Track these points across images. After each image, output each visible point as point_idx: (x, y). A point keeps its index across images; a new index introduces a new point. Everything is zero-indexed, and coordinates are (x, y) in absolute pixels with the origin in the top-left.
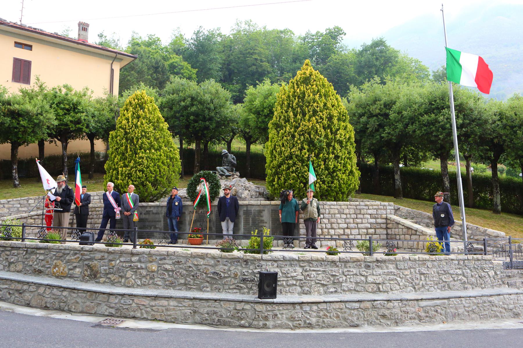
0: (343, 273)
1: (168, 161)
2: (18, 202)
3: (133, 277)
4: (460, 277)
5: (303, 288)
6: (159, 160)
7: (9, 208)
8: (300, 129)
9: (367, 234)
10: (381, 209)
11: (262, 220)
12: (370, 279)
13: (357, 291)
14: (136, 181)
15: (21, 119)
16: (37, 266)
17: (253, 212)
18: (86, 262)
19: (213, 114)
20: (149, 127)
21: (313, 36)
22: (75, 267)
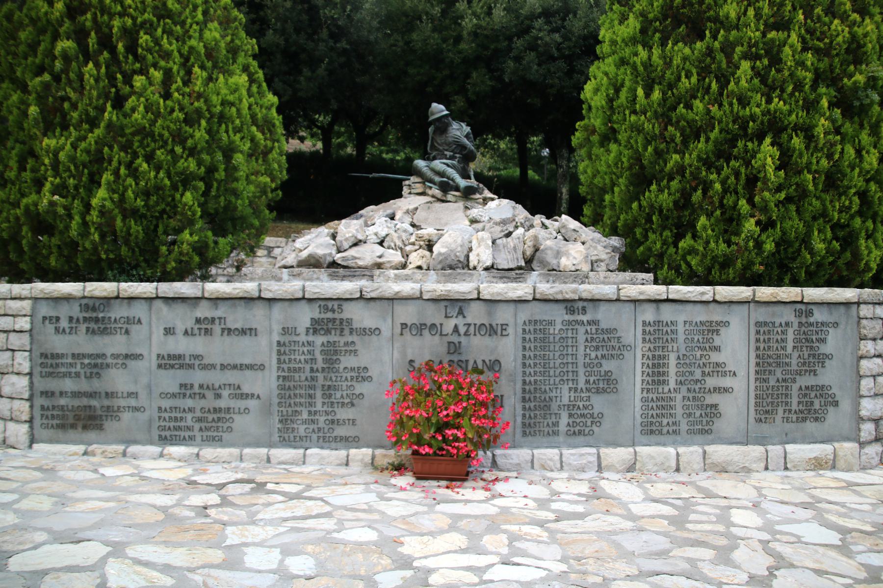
11: (718, 365)
17: (681, 328)
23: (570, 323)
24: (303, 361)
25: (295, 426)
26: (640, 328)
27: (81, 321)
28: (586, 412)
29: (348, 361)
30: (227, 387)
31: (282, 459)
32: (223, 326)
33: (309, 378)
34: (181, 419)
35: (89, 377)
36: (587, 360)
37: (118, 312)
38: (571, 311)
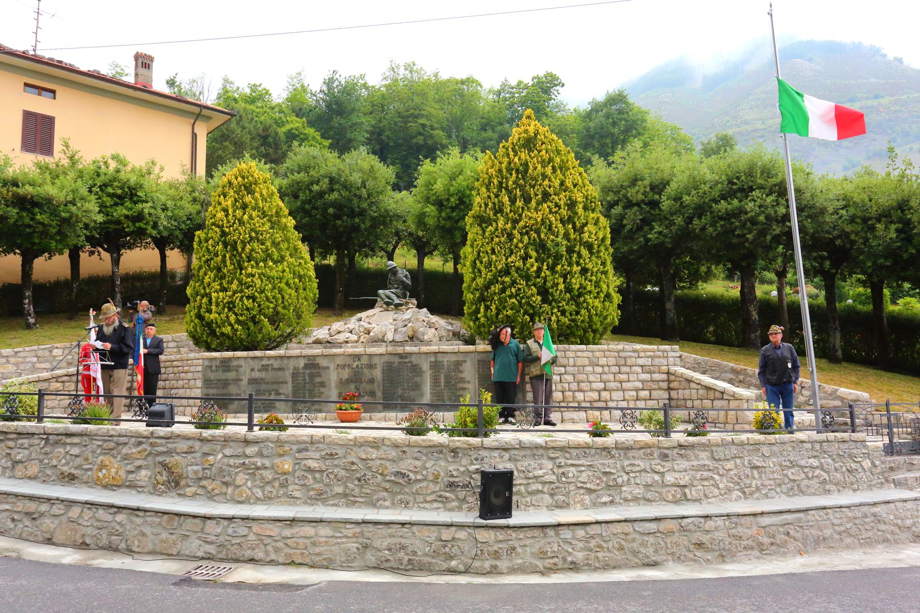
0: (623, 467)
1: (297, 280)
2: (33, 353)
3: (249, 484)
4: (817, 472)
5: (556, 498)
6: (281, 279)
7: (17, 364)
8: (522, 223)
9: (637, 399)
10: (659, 357)
12: (670, 478)
13: (649, 500)
14: (242, 315)
15: (37, 210)
16: (65, 468)
17: (445, 364)
18: (160, 459)
19: (365, 205)
20: (263, 224)
21: (513, 88)
22: (139, 467)
29: (318, 380)
35: (223, 388)
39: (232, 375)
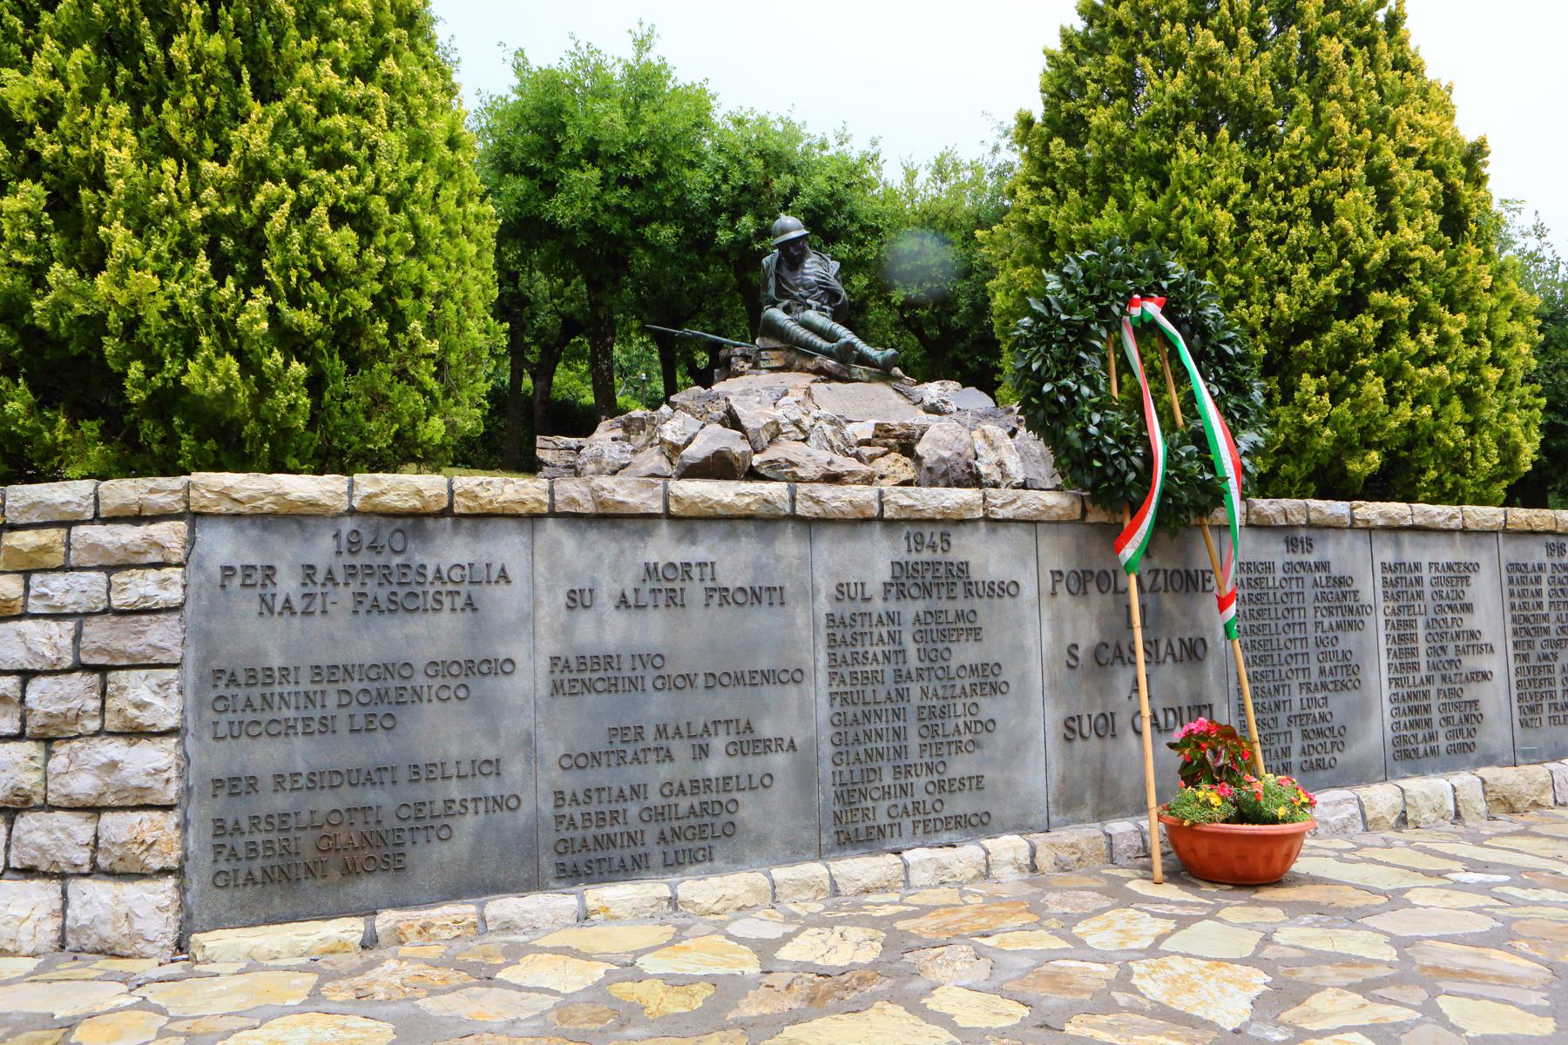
11: (1473, 635)
14: (296, 301)
17: (1426, 574)
23: (1289, 567)
24: (880, 657)
25: (870, 803)
26: (1379, 575)
27: (340, 578)
28: (1324, 725)
29: (965, 653)
30: (722, 728)
31: (866, 881)
32: (709, 584)
33: (893, 694)
34: (614, 815)
36: (1319, 633)
37: (451, 551)
38: (1292, 544)
39: (432, 635)
